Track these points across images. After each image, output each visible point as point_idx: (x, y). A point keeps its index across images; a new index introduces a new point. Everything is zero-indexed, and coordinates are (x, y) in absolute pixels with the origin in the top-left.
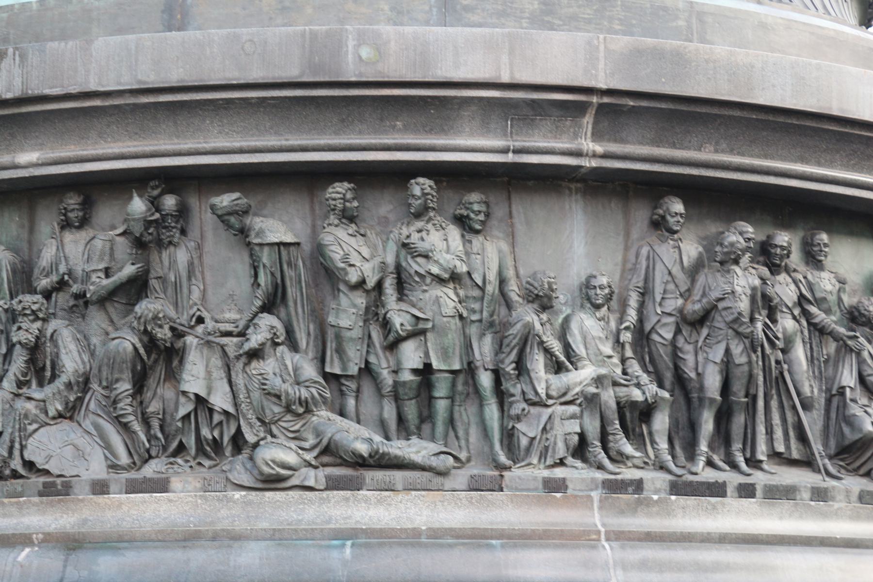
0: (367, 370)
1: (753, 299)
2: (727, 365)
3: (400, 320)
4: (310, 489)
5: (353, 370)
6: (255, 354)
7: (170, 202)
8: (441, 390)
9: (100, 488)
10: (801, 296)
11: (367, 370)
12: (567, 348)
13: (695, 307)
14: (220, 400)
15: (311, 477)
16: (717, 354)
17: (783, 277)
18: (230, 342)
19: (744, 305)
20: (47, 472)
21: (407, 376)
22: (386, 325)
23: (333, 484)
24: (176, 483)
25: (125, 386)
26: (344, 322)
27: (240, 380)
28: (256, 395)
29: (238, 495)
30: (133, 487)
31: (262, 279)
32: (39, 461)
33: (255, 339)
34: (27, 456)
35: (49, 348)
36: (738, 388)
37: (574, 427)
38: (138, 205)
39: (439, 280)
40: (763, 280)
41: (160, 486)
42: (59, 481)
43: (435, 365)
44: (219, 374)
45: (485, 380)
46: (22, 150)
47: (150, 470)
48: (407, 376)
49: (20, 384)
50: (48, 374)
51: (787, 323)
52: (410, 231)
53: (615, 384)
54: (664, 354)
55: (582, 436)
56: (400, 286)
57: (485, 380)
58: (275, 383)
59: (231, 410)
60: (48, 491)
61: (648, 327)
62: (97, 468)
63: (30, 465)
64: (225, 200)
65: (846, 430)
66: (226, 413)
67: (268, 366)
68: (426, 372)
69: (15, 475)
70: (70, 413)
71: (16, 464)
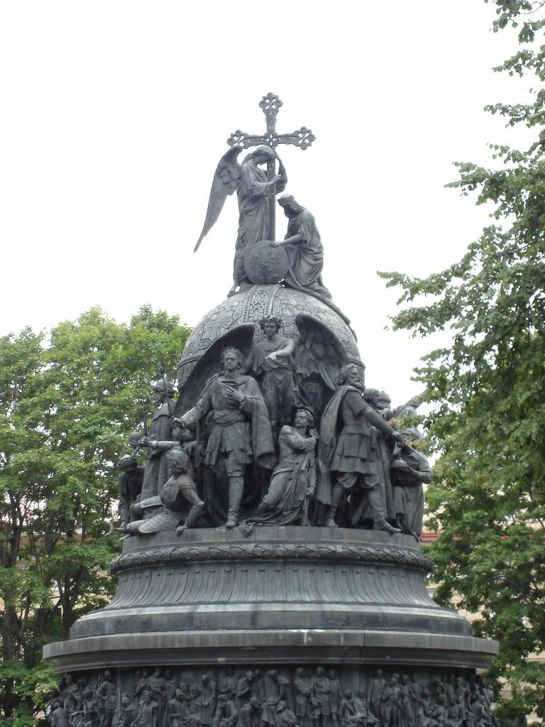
0: (306, 715)
1: (399, 695)
2: (392, 713)
3: (315, 703)
5: (303, 715)
6: (280, 712)
7: (257, 672)
8: (325, 720)
10: (410, 692)
11: (306, 715)
12: (354, 709)
13: (384, 697)
14: (272, 722)
16: (389, 709)
17: (406, 687)
18: (273, 708)
19: (396, 697)
21: (316, 717)
22: (311, 704)
25: (248, 719)
26: (302, 703)
27: (276, 718)
31: (281, 691)
33: (280, 708)
35: (228, 709)
36: (395, 716)
38: (250, 674)
39: (324, 693)
40: (401, 688)
43: (324, 714)
44: (271, 716)
45: (335, 717)
46: (219, 657)
48: (316, 717)
49: (221, 717)
51: (406, 699)
53: (367, 718)
54: (377, 709)
56: (314, 694)
57: (335, 717)
58: (286, 719)
61: (373, 702)
64: (273, 672)
67: (283, 714)
68: (321, 716)
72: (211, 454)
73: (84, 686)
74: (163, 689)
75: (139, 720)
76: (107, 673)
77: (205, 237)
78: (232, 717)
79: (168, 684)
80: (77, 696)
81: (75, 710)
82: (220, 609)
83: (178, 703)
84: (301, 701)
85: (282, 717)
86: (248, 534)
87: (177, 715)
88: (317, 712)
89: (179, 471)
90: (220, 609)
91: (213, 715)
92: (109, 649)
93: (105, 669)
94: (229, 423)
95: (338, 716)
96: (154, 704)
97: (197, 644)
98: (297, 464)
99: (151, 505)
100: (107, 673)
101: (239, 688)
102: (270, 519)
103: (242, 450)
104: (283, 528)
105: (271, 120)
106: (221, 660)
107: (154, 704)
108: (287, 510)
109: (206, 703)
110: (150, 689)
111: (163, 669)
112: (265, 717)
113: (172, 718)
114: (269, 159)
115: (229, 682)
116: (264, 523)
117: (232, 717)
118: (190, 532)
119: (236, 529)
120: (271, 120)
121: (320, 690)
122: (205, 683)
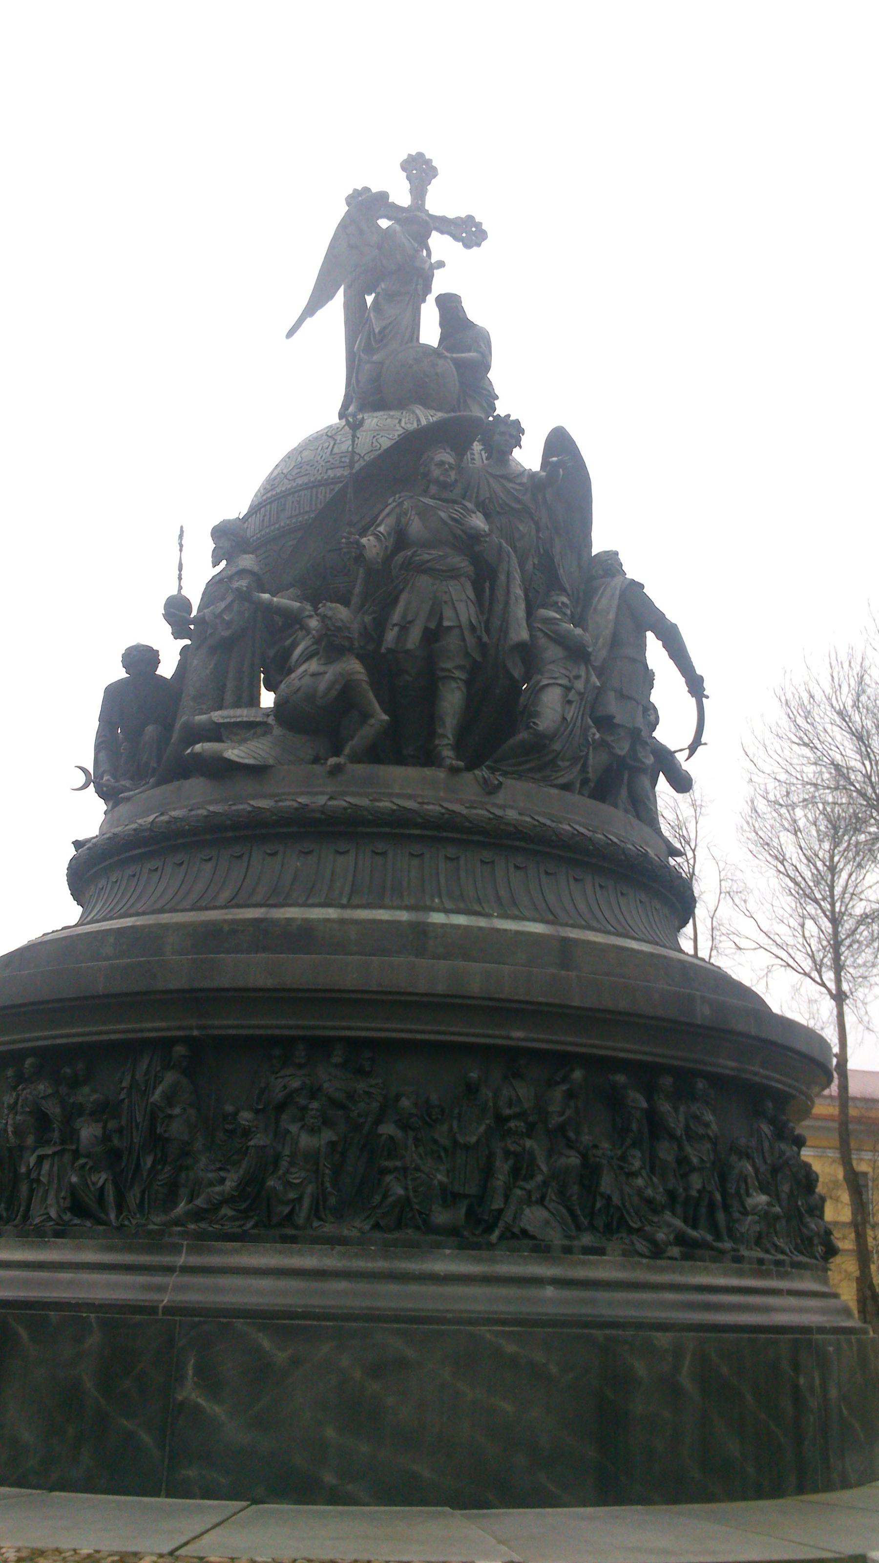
3: (695, 1160)
4: (675, 1259)
9: (567, 1250)
14: (616, 1200)
15: (675, 1251)
20: (533, 1238)
21: (694, 1193)
23: (685, 1257)
24: (609, 1249)
28: (636, 1200)
29: (644, 1261)
30: (588, 1250)
32: (530, 1228)
34: (522, 1225)
37: (757, 1228)
41: (601, 1252)
42: (542, 1243)
47: (587, 1239)
48: (694, 1193)
50: (524, 1172)
52: (695, 1108)
55: (760, 1234)
59: (619, 1204)
60: (536, 1249)
62: (556, 1237)
63: (525, 1233)
64: (621, 1079)
65: (805, 1231)
66: (618, 1208)
67: (640, 1182)
69: (514, 1236)
70: (541, 1201)
71: (516, 1230)
72: (404, 628)
73: (75, 1083)
74: (351, 1096)
75: (288, 1171)
76: (180, 1050)
77: (308, 319)
78: (540, 1178)
79: (361, 1086)
80: (53, 1109)
81: (42, 1142)
82: (482, 922)
83: (398, 1134)
84: (666, 1152)
85: (640, 1192)
86: (491, 790)
87: (399, 1164)
88: (696, 1182)
89: (346, 643)
90: (482, 922)
91: (488, 1172)
92: (216, 984)
93: (174, 1041)
94: (453, 574)
95: (724, 1194)
96: (328, 1135)
97: (475, 987)
98: (577, 677)
99: (238, 720)
100: (180, 1050)
101: (554, 1108)
102: (531, 770)
103: (473, 628)
104: (555, 791)
105: (419, 190)
106: (518, 1035)
107: (328, 1135)
108: (563, 760)
109: (474, 1139)
110: (314, 1092)
111: (354, 1045)
112: (607, 1183)
113: (385, 1171)
114: (423, 241)
115: (524, 1091)
116: (520, 776)
117: (540, 1178)
118: (360, 769)
119: (468, 776)
120: (419, 190)
121: (701, 1131)
122: (472, 1089)
